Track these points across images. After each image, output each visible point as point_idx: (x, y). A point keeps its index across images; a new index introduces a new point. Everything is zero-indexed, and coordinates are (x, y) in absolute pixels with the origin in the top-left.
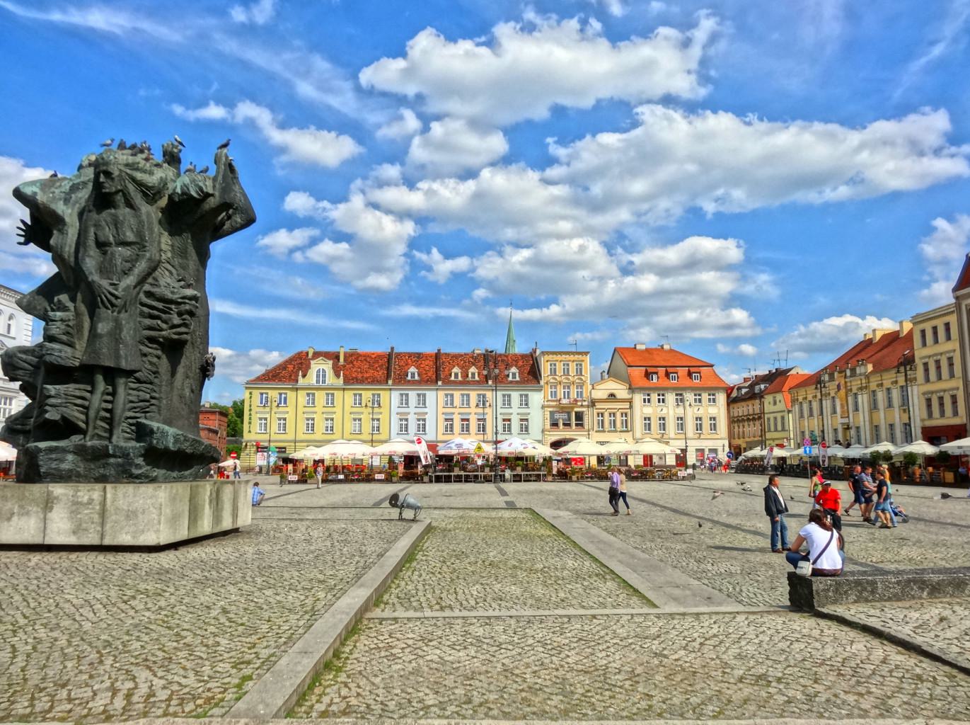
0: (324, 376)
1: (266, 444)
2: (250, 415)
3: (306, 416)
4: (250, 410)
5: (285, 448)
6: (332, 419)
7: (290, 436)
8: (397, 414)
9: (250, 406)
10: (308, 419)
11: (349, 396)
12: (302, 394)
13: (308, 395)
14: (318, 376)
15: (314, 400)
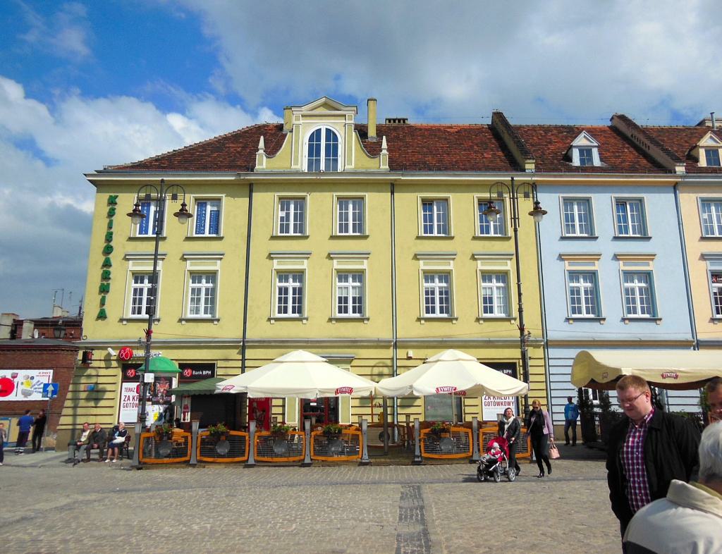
0: (332, 150)
1: (140, 353)
2: (107, 264)
3: (277, 265)
4: (108, 250)
5: (211, 367)
6: (359, 276)
7: (229, 330)
8: (561, 257)
9: (109, 238)
10: (283, 275)
11: (409, 202)
12: (266, 201)
13: (284, 202)
14: (314, 150)
15: (300, 217)
